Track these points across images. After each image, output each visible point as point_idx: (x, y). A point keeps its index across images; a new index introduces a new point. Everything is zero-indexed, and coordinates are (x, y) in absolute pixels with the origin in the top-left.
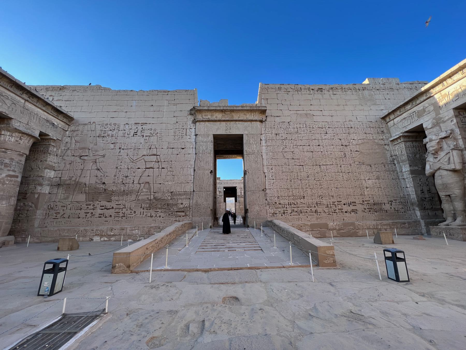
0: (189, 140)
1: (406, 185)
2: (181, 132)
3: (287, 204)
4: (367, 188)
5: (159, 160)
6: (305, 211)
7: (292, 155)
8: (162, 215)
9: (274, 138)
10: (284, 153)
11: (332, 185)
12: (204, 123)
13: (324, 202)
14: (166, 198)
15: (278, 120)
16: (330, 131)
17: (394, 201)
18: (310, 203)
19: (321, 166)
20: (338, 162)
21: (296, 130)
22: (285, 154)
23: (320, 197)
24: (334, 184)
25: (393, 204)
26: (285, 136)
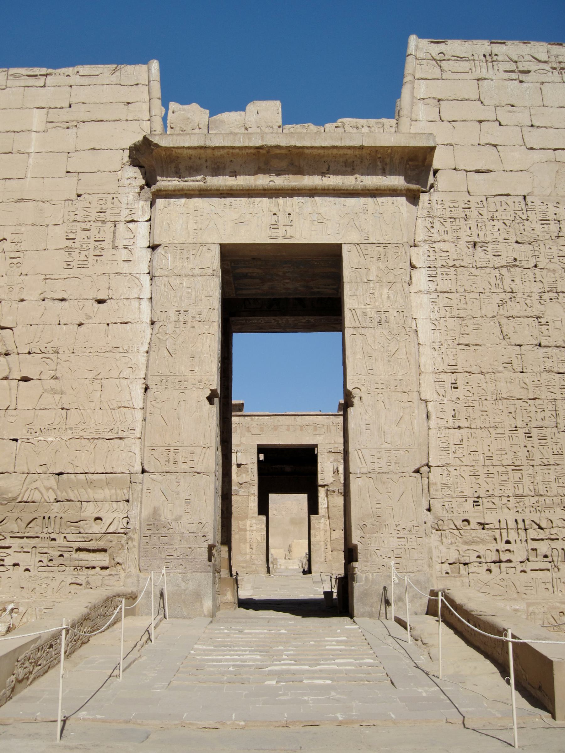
0: (126, 268)
2: (93, 234)
3: (512, 524)
5: (11, 347)
7: (536, 332)
8: (25, 560)
9: (467, 260)
10: (504, 321)
12: (183, 200)
14: (37, 496)
15: (481, 185)
21: (553, 227)
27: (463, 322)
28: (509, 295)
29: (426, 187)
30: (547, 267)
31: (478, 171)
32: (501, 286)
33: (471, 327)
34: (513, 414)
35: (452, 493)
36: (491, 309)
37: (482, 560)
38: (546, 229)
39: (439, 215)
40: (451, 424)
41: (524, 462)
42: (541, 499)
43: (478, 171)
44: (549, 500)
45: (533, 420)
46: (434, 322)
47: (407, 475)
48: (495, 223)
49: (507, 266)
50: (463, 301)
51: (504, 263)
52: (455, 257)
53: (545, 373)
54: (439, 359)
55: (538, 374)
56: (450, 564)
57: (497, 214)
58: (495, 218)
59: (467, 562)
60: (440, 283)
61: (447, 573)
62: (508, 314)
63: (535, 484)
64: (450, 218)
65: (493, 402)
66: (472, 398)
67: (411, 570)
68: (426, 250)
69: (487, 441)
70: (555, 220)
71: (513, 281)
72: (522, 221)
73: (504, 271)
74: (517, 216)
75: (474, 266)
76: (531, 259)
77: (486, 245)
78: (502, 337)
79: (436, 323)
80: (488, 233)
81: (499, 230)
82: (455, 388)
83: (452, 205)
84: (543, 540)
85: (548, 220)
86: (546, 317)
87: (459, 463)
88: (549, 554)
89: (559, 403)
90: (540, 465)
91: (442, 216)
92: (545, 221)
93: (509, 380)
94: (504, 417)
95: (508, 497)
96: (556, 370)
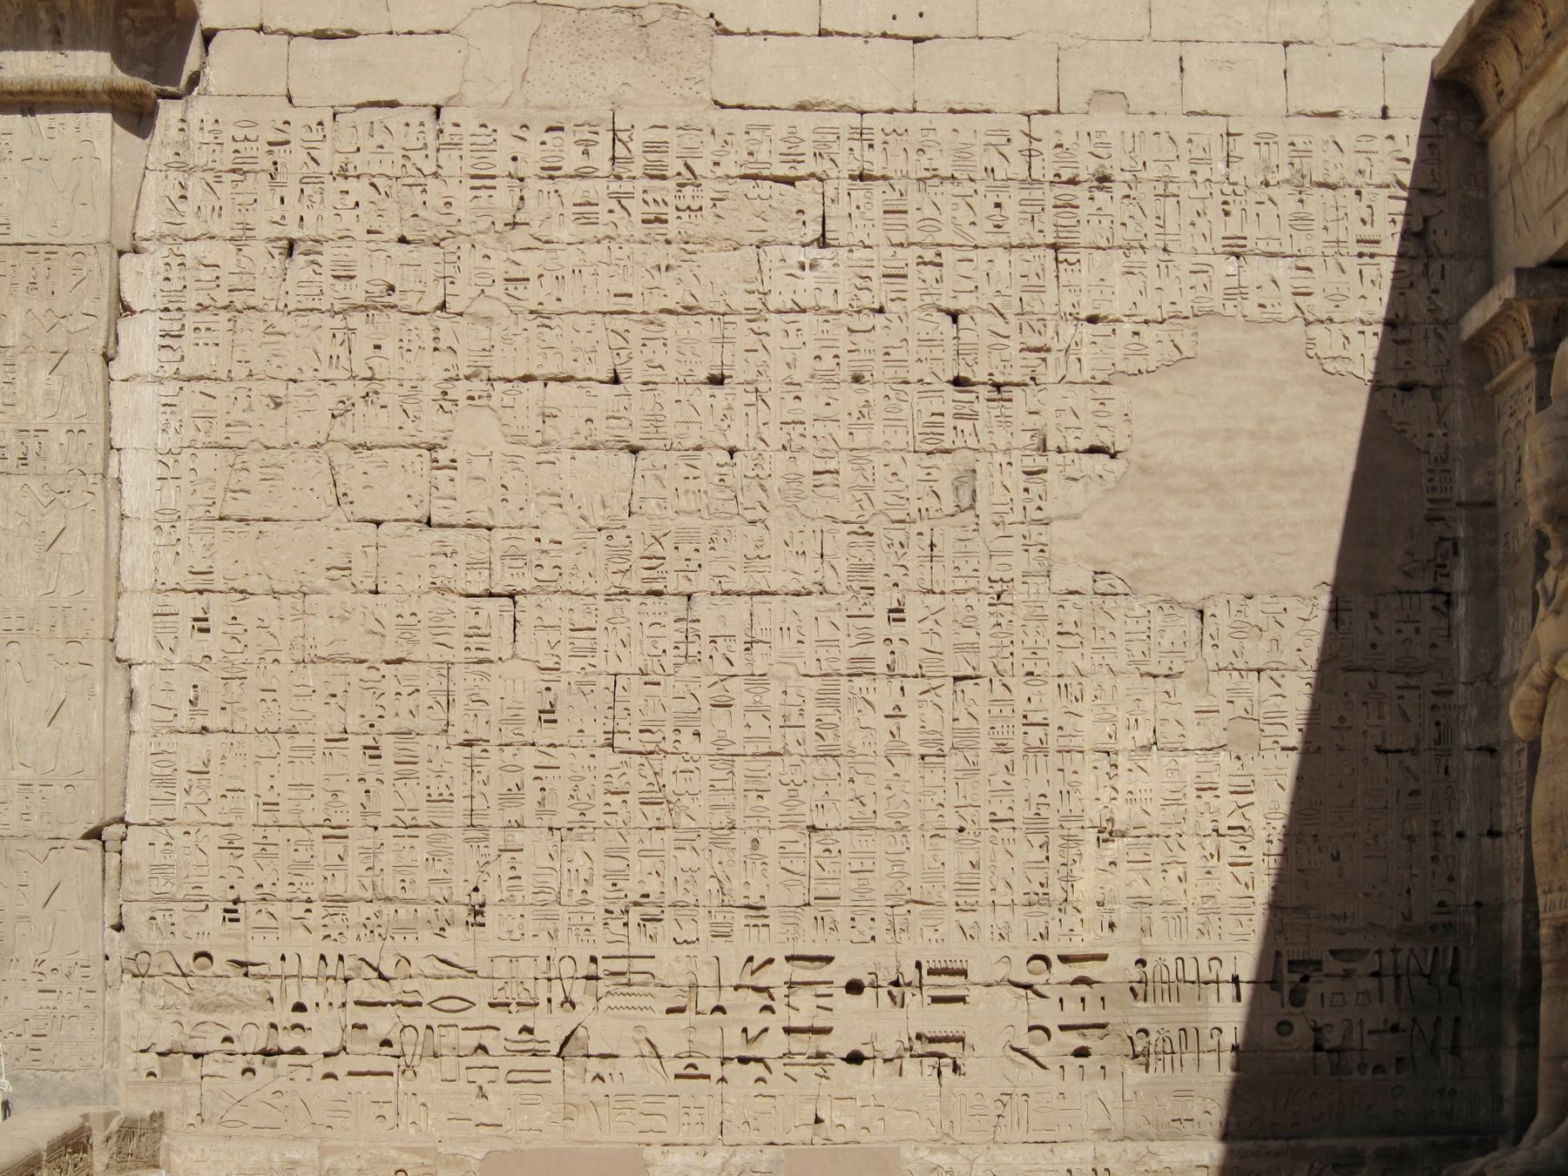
1: (1494, 806)
3: (310, 965)
4: (1107, 834)
6: (473, 1039)
7: (421, 487)
9: (264, 291)
10: (342, 457)
11: (774, 803)
13: (669, 962)
15: (326, 75)
16: (859, 217)
17: (1332, 965)
18: (527, 969)
19: (701, 606)
20: (883, 562)
22: (353, 469)
23: (635, 916)
24: (793, 788)
25: (1313, 991)
26: (373, 270)
27: (239, 460)
28: (362, 387)
29: (177, 83)
30: (471, 310)
31: (321, 35)
32: (344, 362)
33: (257, 473)
34: (340, 700)
35: (174, 890)
36: (310, 427)
37: (236, 1047)
38: (483, 202)
39: (203, 162)
40: (183, 722)
41: (354, 816)
42: (391, 907)
43: (321, 35)
44: (405, 912)
45: (390, 711)
46: (166, 457)
47: (69, 844)
48: (351, 184)
49: (366, 308)
50: (243, 402)
51: (359, 298)
52: (235, 281)
53: (434, 594)
54: (170, 556)
55: (415, 597)
56: (160, 1054)
57: (356, 159)
58: (351, 172)
59: (200, 1050)
60: (190, 353)
61: (151, 1074)
62: (356, 439)
63: (377, 871)
64: (234, 171)
65: (292, 667)
66: (242, 658)
67: (66, 1066)
68: (161, 263)
69: (269, 766)
70: (510, 175)
71: (378, 347)
72: (422, 180)
73: (356, 319)
74: (408, 164)
75: (281, 306)
76: (431, 284)
77: (318, 248)
78: (332, 500)
79: (170, 460)
80: (328, 214)
81: (357, 204)
82: (201, 630)
83: (240, 137)
84: (384, 1004)
85: (493, 177)
86: (451, 447)
87: (194, 815)
88: (393, 1037)
89: (456, 671)
90: (394, 826)
91: (211, 165)
92: (482, 180)
93: (337, 612)
94: (315, 705)
95: (309, 901)
96: (460, 586)
